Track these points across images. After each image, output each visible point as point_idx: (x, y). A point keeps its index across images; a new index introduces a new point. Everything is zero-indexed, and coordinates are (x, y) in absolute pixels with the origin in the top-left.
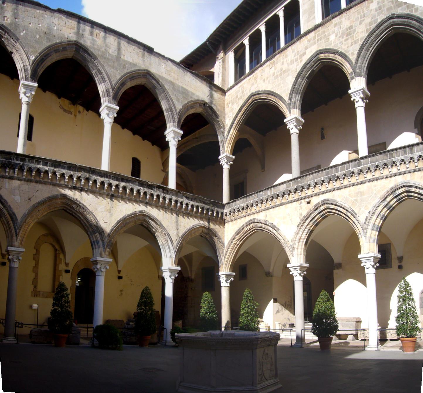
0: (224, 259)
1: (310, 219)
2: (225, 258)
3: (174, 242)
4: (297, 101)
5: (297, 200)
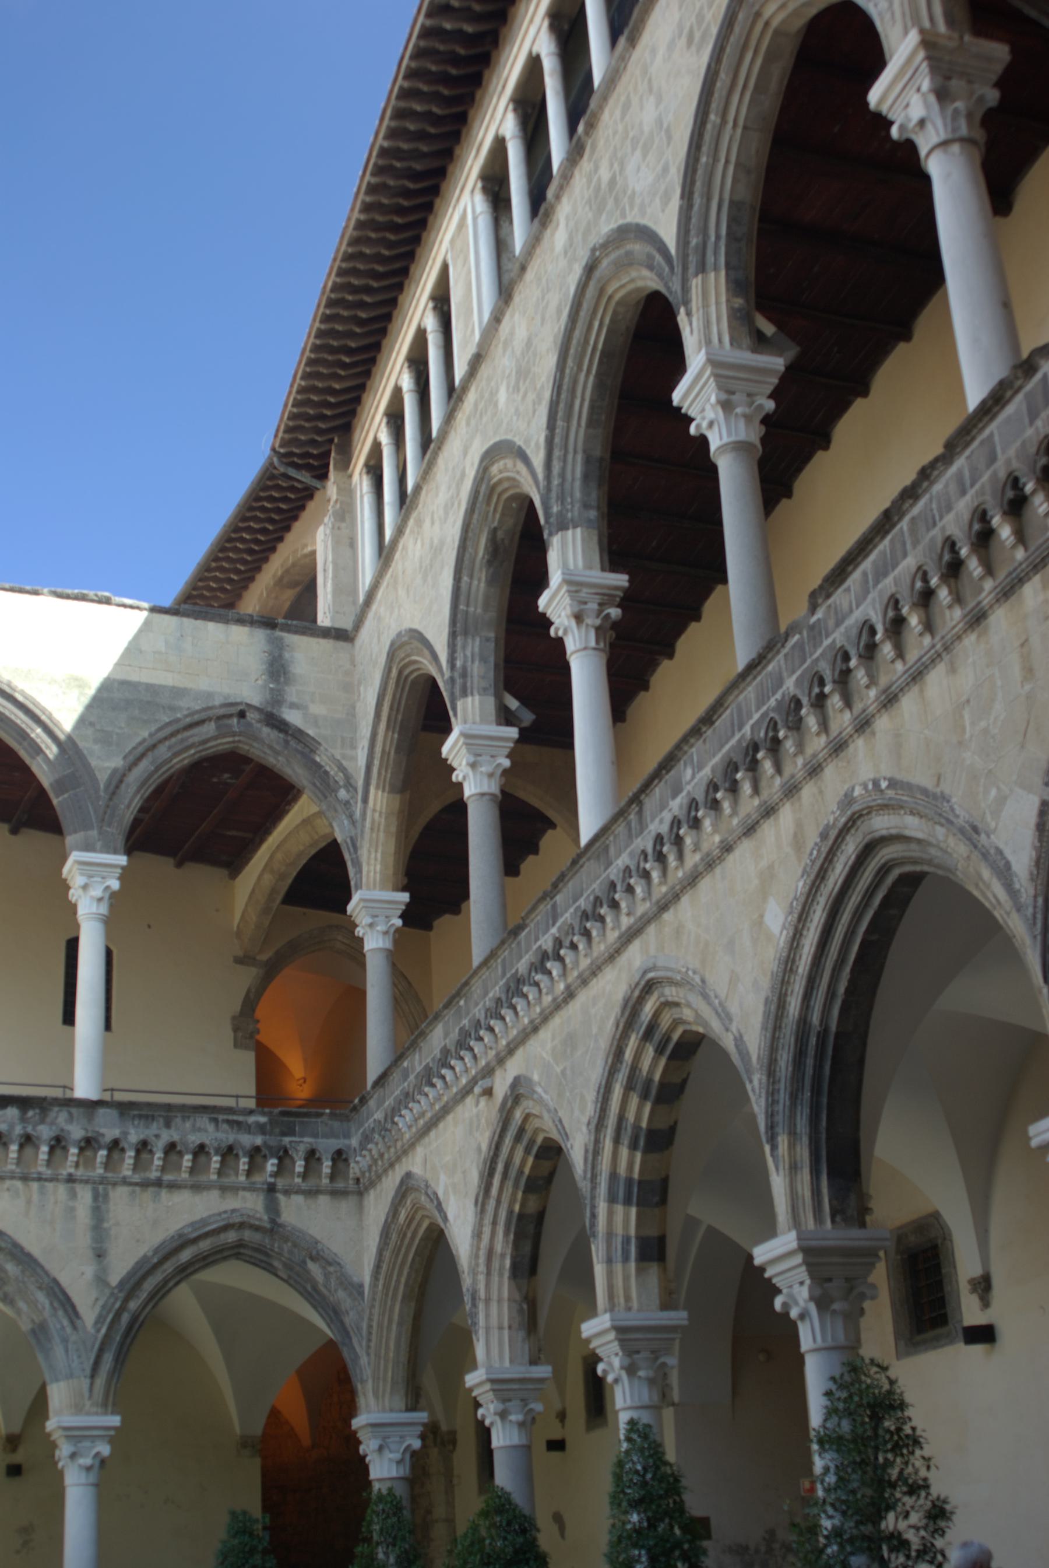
0: (368, 1354)
1: (500, 1167)
2: (368, 1347)
3: (82, 1309)
4: (469, 663)
5: (468, 1088)
